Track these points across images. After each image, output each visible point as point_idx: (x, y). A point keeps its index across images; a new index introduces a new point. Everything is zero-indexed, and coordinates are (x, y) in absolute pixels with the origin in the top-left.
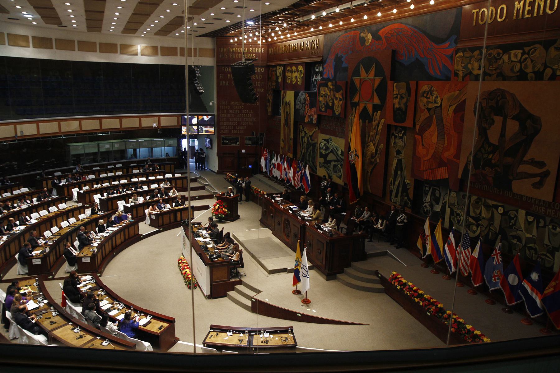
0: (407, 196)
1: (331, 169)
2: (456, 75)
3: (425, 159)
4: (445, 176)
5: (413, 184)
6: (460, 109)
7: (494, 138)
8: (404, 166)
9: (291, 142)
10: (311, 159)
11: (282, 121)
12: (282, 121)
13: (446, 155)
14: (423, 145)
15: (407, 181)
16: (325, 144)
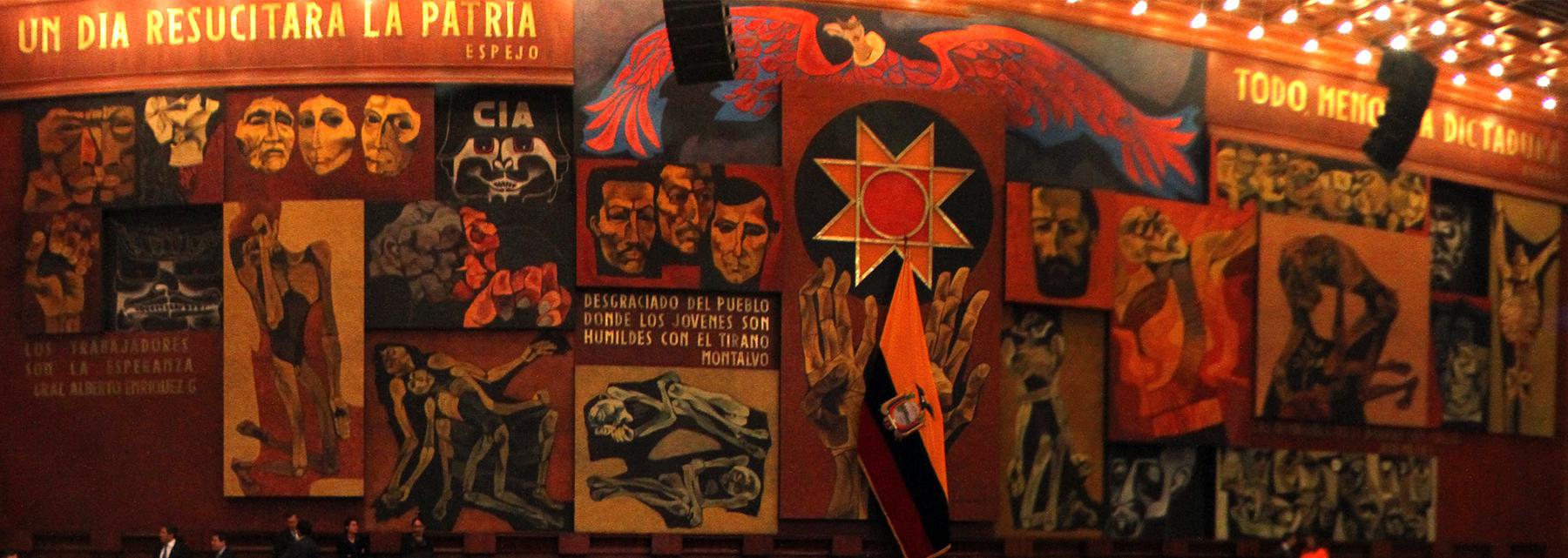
0: (1083, 496)
1: (686, 494)
2: (1223, 194)
3: (1152, 387)
4: (1216, 418)
5: (1099, 463)
6: (1245, 268)
7: (1323, 325)
8: (1060, 419)
9: (345, 428)
10: (500, 481)
11: (242, 334)
12: (242, 334)
13: (1213, 370)
14: (1141, 352)
15: (1078, 457)
16: (629, 405)
